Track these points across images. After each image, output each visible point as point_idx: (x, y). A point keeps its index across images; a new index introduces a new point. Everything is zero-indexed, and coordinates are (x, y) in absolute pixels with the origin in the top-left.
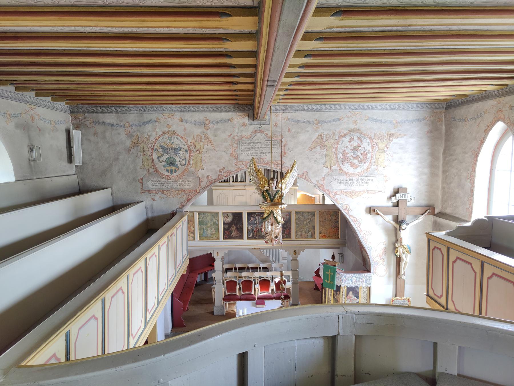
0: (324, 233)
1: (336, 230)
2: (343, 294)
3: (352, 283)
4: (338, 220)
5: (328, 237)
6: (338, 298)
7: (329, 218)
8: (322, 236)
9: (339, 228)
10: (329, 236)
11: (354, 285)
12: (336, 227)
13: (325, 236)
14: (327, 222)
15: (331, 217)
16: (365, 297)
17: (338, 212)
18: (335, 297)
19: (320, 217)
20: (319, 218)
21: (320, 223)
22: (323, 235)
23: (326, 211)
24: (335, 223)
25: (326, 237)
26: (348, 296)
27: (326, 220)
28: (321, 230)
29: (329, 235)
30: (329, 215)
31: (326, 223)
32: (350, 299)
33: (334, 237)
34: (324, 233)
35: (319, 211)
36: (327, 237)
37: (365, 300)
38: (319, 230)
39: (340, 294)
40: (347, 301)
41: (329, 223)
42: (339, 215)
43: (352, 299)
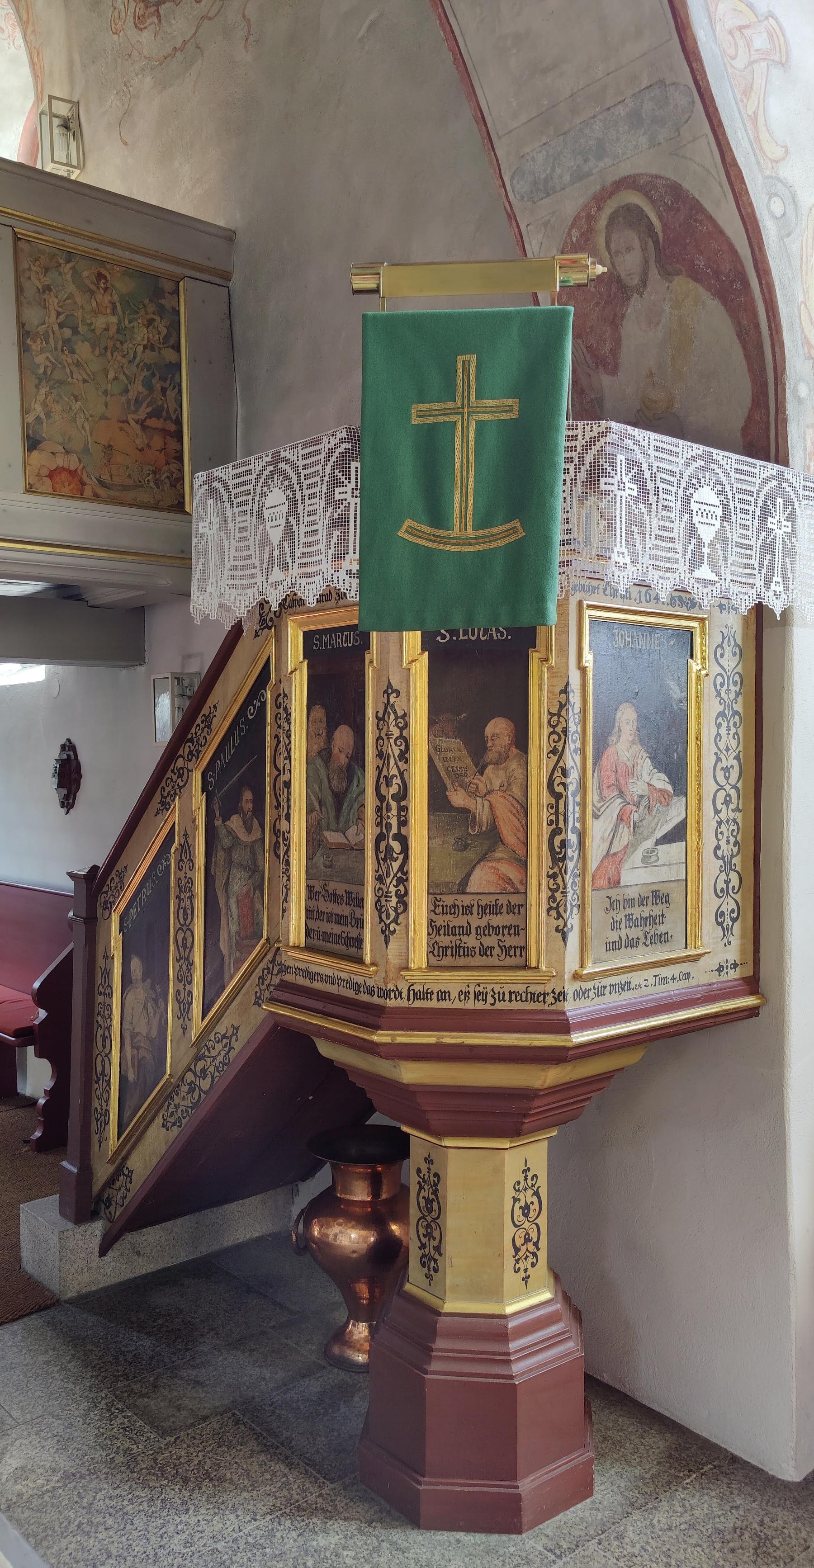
0: (67, 452)
1: (158, 441)
2: (559, 733)
3: (695, 562)
4: (169, 355)
5: (101, 491)
6: (496, 798)
7: (100, 322)
8: (51, 475)
9: (179, 422)
10: (102, 483)
11: (706, 583)
12: (156, 413)
13: (73, 473)
14: (83, 350)
15: (114, 319)
16: (726, 770)
17: (168, 286)
18: (458, 798)
19: (19, 290)
20: (19, 305)
21: (24, 349)
22: (60, 461)
23: (70, 256)
24: (145, 373)
25: (83, 484)
26: (604, 761)
27: (75, 331)
28: (38, 418)
29: (106, 478)
30: (99, 297)
31: (78, 364)
32: (621, 794)
33: (143, 496)
34: (67, 452)
35: (16, 238)
36: (88, 492)
37: (727, 803)
38: (25, 410)
39: (521, 741)
40: (596, 816)
41: (106, 372)
42: (178, 313)
43: (637, 788)
